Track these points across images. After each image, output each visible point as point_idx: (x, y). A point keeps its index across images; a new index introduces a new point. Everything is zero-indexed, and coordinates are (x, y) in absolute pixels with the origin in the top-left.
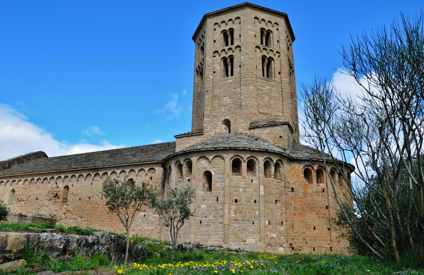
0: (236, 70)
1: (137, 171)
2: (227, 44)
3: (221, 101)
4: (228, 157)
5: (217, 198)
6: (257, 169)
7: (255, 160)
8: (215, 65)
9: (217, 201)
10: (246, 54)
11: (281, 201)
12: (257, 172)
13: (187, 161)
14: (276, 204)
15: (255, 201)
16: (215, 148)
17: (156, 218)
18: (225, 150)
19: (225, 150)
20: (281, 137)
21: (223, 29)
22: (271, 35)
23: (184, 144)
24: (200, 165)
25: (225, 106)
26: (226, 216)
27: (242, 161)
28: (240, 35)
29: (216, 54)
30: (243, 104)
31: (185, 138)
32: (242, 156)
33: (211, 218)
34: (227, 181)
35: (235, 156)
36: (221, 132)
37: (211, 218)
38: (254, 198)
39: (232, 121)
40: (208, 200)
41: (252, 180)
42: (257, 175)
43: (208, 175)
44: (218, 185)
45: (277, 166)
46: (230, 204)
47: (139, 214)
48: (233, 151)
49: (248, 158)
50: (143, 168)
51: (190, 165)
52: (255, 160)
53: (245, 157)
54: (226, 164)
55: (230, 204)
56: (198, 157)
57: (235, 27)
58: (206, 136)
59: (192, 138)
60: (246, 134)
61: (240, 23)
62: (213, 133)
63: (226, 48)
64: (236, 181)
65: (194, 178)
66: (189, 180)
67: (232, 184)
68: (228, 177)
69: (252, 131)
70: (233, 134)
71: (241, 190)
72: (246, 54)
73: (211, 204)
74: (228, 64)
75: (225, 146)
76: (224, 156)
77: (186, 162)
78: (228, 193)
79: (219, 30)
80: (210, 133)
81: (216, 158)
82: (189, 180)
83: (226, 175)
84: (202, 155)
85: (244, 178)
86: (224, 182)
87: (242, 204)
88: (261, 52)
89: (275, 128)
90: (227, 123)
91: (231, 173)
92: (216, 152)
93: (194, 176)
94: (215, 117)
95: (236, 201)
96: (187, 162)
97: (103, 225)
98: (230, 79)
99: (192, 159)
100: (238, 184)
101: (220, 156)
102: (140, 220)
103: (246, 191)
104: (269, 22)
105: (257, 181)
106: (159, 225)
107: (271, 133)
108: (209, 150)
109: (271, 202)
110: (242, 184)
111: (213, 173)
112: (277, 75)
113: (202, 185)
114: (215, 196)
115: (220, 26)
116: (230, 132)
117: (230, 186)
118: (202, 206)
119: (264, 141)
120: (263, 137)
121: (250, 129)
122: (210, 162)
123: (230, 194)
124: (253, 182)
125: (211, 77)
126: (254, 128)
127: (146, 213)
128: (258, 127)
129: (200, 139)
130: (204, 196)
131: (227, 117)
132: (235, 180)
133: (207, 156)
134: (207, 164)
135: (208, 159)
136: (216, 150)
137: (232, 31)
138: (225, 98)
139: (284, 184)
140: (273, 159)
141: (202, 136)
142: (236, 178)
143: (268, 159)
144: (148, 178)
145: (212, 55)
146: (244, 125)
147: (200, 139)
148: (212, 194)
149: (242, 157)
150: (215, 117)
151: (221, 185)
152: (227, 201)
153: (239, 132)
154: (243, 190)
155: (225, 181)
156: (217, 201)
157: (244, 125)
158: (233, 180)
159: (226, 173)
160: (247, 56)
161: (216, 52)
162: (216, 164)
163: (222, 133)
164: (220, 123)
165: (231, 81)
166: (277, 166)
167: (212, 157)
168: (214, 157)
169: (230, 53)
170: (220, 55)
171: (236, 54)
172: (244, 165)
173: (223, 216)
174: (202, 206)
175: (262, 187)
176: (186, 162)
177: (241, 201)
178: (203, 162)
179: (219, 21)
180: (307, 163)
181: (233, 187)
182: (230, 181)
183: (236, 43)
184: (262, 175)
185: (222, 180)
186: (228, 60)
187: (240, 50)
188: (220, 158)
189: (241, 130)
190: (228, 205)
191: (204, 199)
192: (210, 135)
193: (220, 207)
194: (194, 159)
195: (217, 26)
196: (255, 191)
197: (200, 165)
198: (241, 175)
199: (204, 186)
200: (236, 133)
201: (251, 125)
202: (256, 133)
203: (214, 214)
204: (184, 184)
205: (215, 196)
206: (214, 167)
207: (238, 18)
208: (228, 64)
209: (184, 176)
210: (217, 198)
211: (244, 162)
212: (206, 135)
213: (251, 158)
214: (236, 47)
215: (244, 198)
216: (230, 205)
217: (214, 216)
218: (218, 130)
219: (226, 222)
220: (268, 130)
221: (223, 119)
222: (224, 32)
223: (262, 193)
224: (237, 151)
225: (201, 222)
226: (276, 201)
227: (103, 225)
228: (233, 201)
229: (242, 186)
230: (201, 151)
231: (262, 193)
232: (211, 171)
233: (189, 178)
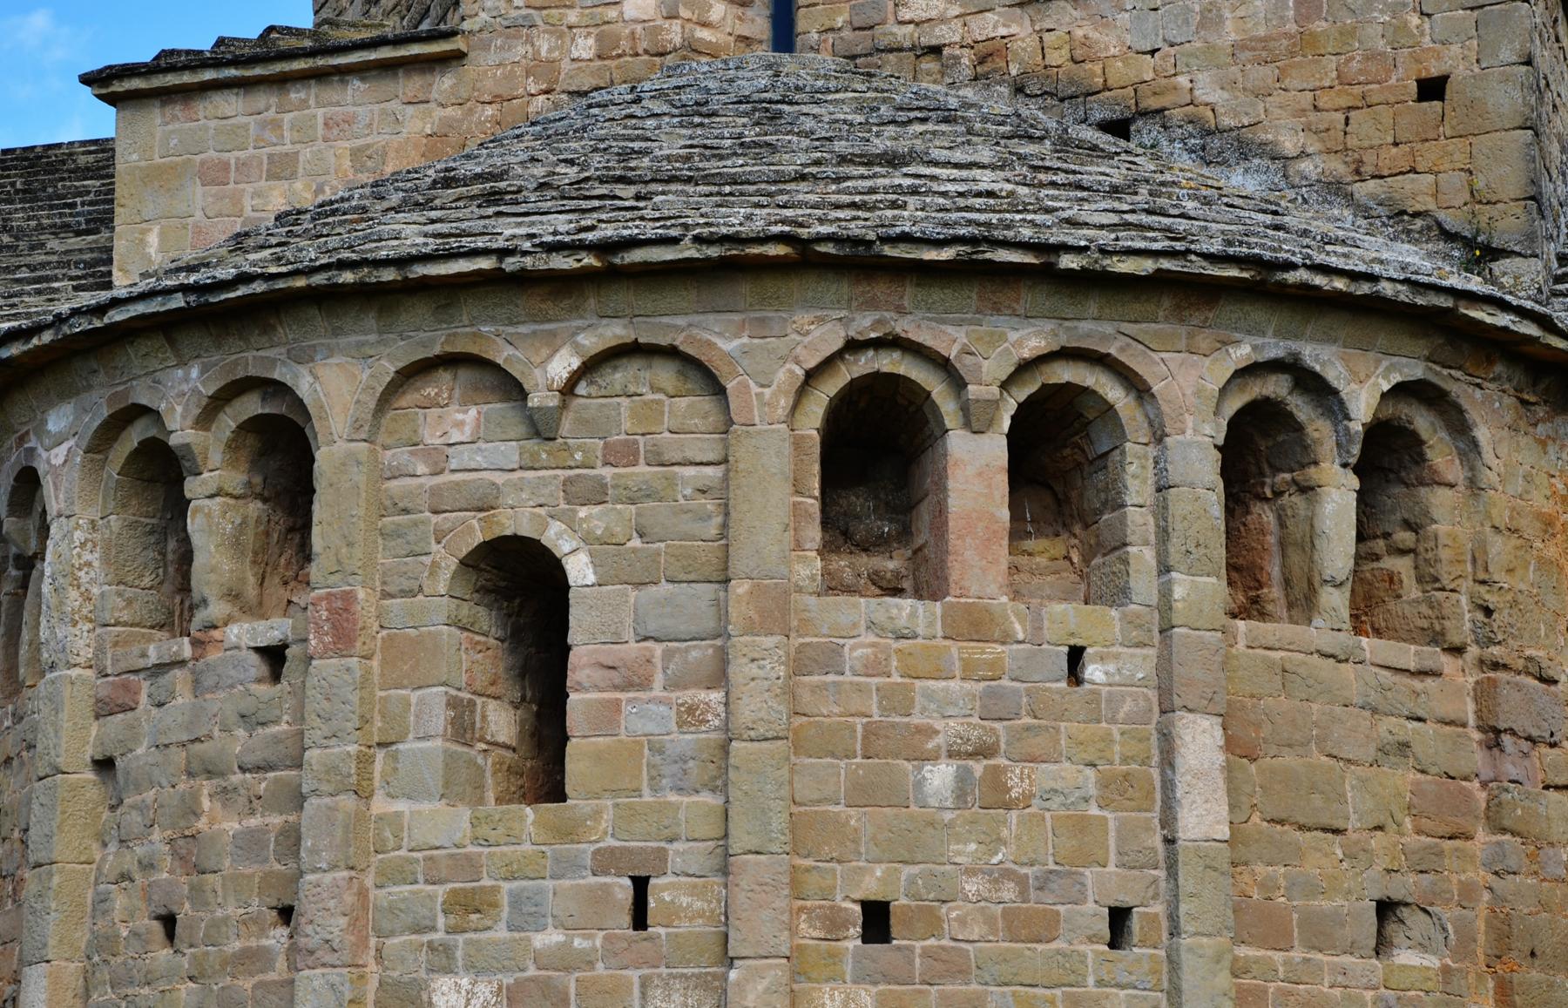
5: (641, 885)
6: (1138, 519)
7: (1114, 393)
9: (640, 919)
11: (1448, 914)
12: (1142, 555)
13: (251, 406)
14: (1382, 946)
15: (1119, 918)
16: (605, 248)
18: (730, 269)
19: (730, 269)
20: (1432, 89)
23: (214, 175)
24: (417, 466)
27: (948, 407)
31: (229, 105)
32: (949, 339)
34: (760, 666)
35: (853, 346)
36: (674, 34)
38: (1107, 881)
40: (527, 916)
41: (1076, 656)
42: (1143, 584)
44: (649, 715)
45: (1386, 457)
46: (801, 967)
48: (844, 288)
49: (1026, 367)
52: (1114, 393)
53: (992, 352)
54: (742, 454)
55: (799, 965)
56: (388, 368)
58: (489, 86)
59: (313, 106)
60: (988, 56)
62: (585, 47)
64: (874, 668)
65: (344, 636)
66: (274, 656)
67: (829, 711)
68: (776, 612)
70: (827, 61)
71: (940, 776)
73: (564, 960)
75: (734, 219)
76: (720, 336)
77: (228, 422)
78: (779, 822)
80: (544, 45)
81: (619, 376)
83: (740, 588)
84: (428, 335)
85: (974, 626)
86: (719, 676)
87: (950, 966)
91: (809, 567)
92: (621, 297)
93: (343, 607)
95: (877, 921)
96: (253, 426)
99: (304, 386)
100: (897, 700)
101: (671, 353)
103: (997, 797)
105: (1141, 664)
107: (1305, 43)
108: (524, 280)
109: (1320, 934)
110: (948, 706)
111: (579, 570)
113: (439, 718)
114: (605, 862)
116: (784, 36)
117: (802, 739)
119: (1219, 143)
120: (1209, 91)
122: (540, 428)
123: (804, 833)
124: (1093, 671)
130: (470, 866)
132: (857, 651)
133: (502, 355)
134: (509, 452)
135: (514, 390)
136: (611, 273)
139: (1484, 694)
141: (444, 83)
142: (869, 626)
143: (1276, 387)
147: (417, 124)
148: (567, 833)
149: (942, 364)
151: (690, 716)
152: (763, 923)
153: (904, 34)
154: (963, 778)
155: (740, 670)
156: (640, 919)
158: (830, 659)
159: (738, 565)
162: (623, 454)
163: (693, 49)
166: (1386, 457)
167: (562, 365)
168: (592, 366)
172: (974, 466)
175: (1200, 741)
176: (228, 422)
177: (934, 926)
178: (456, 421)
181: (832, 745)
182: (800, 664)
184: (1201, 589)
185: (700, 653)
188: (665, 373)
190: (776, 971)
191: (469, 906)
192: (542, 68)
194: (334, 382)
196: (1116, 789)
197: (417, 466)
198: (926, 580)
199: (463, 727)
200: (862, 42)
202: (1109, 42)
204: (217, 702)
205: (605, 862)
206: (597, 495)
209: (216, 609)
210: (641, 885)
211: (974, 422)
212: (489, 65)
213: (1064, 373)
215: (971, 887)
216: (797, 974)
223: (1203, 816)
224: (881, 289)
226: (1386, 909)
228: (833, 925)
229: (949, 729)
230: (428, 286)
231: (1203, 816)
232: (557, 538)
233: (272, 630)
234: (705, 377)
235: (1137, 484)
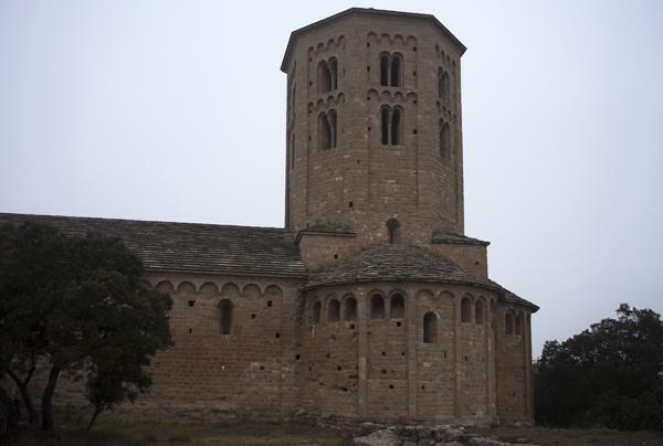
0: (406, 135)
1: (241, 288)
2: (384, 83)
3: (382, 185)
4: (459, 294)
8: (370, 116)
10: (427, 113)
17: (289, 372)
20: (477, 263)
21: (383, 49)
22: (446, 81)
25: (389, 195)
26: (458, 380)
28: (415, 74)
29: (372, 96)
30: (421, 199)
33: (438, 382)
37: (438, 382)
39: (403, 223)
43: (429, 318)
44: (446, 334)
47: (249, 364)
50: (255, 282)
51: (398, 301)
53: (477, 294)
57: (407, 53)
60: (426, 249)
61: (415, 49)
63: (381, 89)
66: (399, 324)
69: (437, 247)
71: (471, 343)
72: (427, 113)
74: (391, 124)
79: (377, 49)
82: (399, 324)
84: (424, 287)
86: (454, 331)
88: (440, 111)
89: (470, 248)
90: (393, 225)
94: (371, 210)
97: (168, 383)
98: (398, 151)
99: (407, 291)
102: (253, 376)
104: (448, 57)
106: (296, 385)
111: (438, 317)
112: (453, 156)
115: (379, 42)
116: (391, 241)
118: (426, 364)
121: (433, 242)
125: (366, 136)
126: (440, 242)
127: (265, 364)
128: (446, 242)
129: (348, 245)
131: (395, 216)
135: (433, 294)
137: (397, 59)
138: (390, 181)
140: (473, 294)
141: (352, 240)
144: (263, 302)
145: (366, 95)
146: (423, 234)
147: (348, 245)
150: (375, 210)
152: (459, 358)
157: (423, 234)
160: (428, 117)
161: (372, 91)
164: (384, 223)
165: (398, 153)
169: (398, 102)
170: (380, 100)
171: (408, 105)
173: (454, 379)
174: (426, 364)
179: (379, 31)
180: (512, 307)
183: (407, 86)
186: (391, 113)
187: (415, 102)
189: (418, 241)
191: (427, 354)
193: (449, 367)
195: (372, 37)
201: (434, 234)
203: (441, 376)
207: (411, 37)
208: (391, 124)
214: (409, 94)
217: (442, 380)
218: (379, 234)
219: (459, 388)
220: (458, 250)
221: (388, 217)
222: (384, 57)
225: (423, 387)
227: (168, 383)
233: (399, 320)
234: (452, 296)
235: (484, 310)
